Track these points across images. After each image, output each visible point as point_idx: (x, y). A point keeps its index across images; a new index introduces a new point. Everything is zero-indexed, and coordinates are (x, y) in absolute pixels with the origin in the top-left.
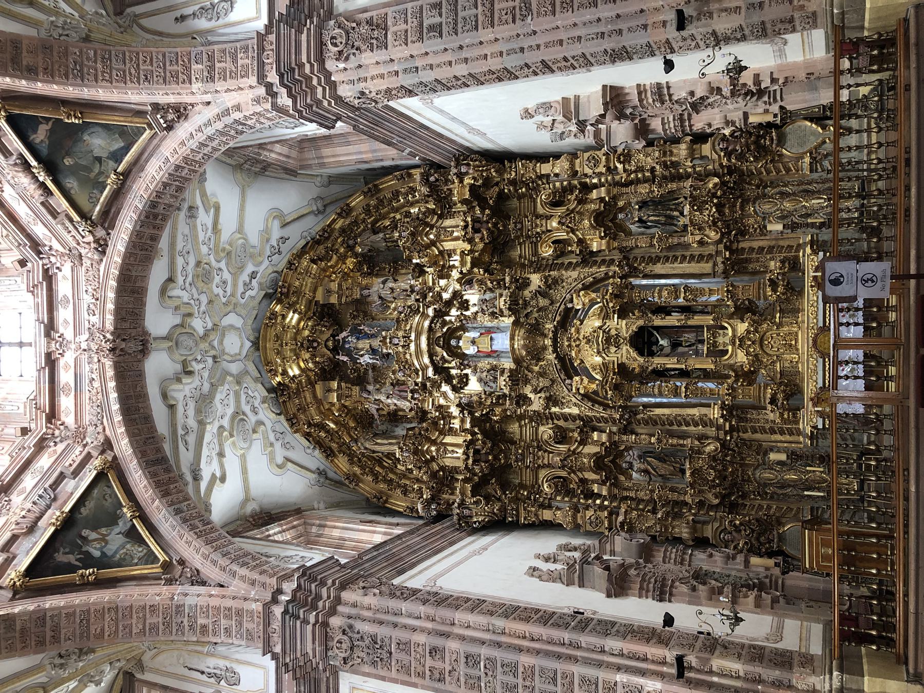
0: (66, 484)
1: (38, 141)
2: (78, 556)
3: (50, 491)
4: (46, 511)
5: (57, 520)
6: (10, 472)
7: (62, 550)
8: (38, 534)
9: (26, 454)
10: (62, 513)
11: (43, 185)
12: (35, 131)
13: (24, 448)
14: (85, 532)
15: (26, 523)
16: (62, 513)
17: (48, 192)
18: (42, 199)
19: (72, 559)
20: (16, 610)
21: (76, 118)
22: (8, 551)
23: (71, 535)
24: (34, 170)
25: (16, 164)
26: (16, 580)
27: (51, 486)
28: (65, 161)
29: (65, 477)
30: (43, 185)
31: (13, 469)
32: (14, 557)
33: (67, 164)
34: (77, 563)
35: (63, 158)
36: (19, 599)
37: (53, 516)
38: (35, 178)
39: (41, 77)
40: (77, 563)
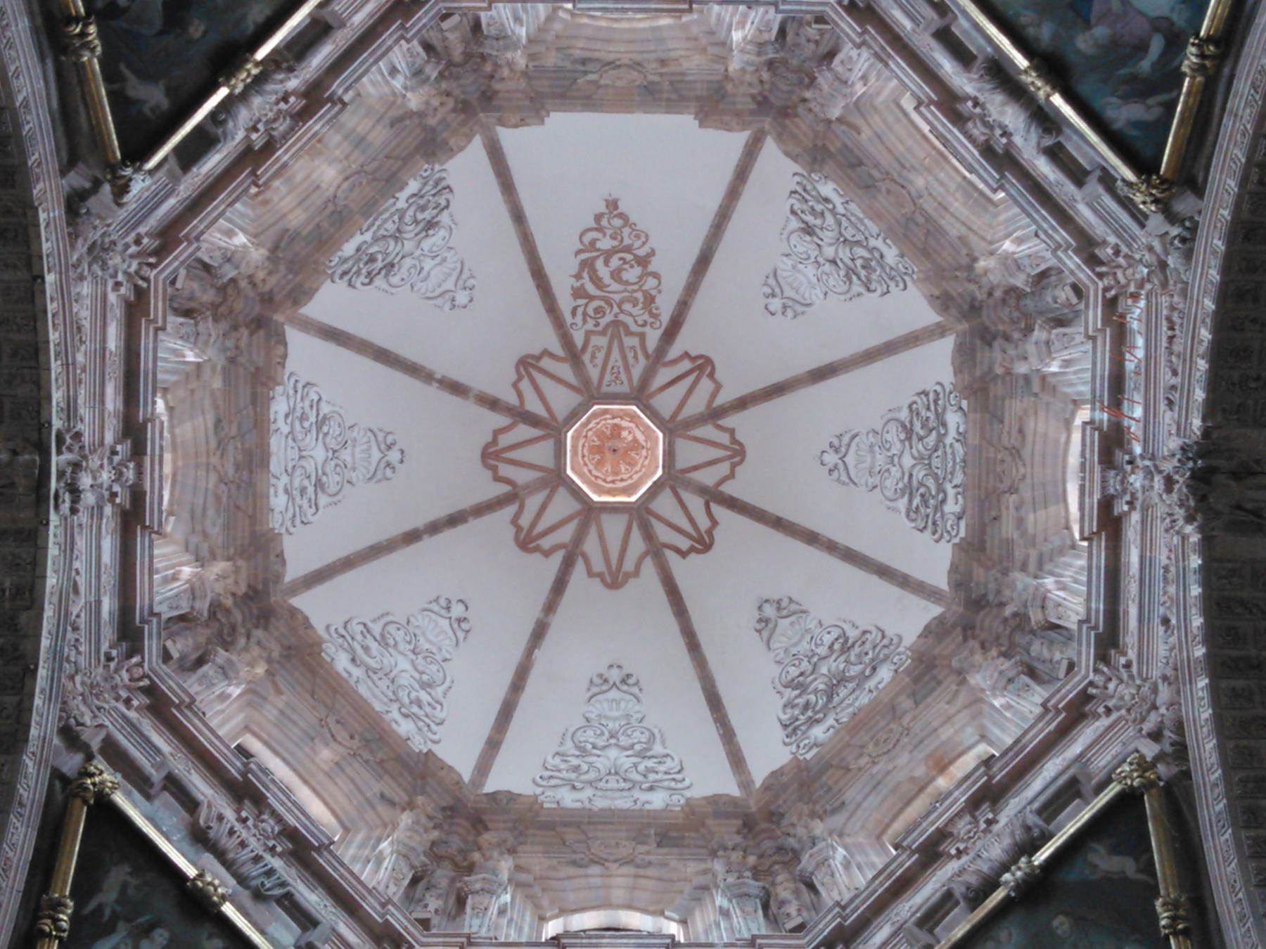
0: (287, 927)
1: (1093, 858)
2: (107, 912)
3: (278, 892)
4: (236, 875)
5: (211, 884)
6: (335, 869)
7: (134, 881)
8: (186, 846)
9: (370, 907)
10: (223, 898)
11: (990, 884)
12: (1115, 850)
13: (383, 905)
14: (161, 936)
15: (218, 832)
16: (223, 898)
17: (976, 896)
18: (959, 891)
19: (108, 896)
20: (29, 764)
21: (1174, 919)
22: (165, 788)
23: (164, 904)
24: (1023, 859)
25: (1028, 829)
26: (97, 779)
27: (289, 896)
28: (1061, 918)
29: (304, 929)
30: (990, 884)
31: (341, 876)
32: (148, 797)
33: (1055, 923)
34: (92, 905)
35: (1066, 914)
36: (51, 786)
37: (219, 881)
38: (1005, 868)
39: (1244, 834)
40: (92, 905)
